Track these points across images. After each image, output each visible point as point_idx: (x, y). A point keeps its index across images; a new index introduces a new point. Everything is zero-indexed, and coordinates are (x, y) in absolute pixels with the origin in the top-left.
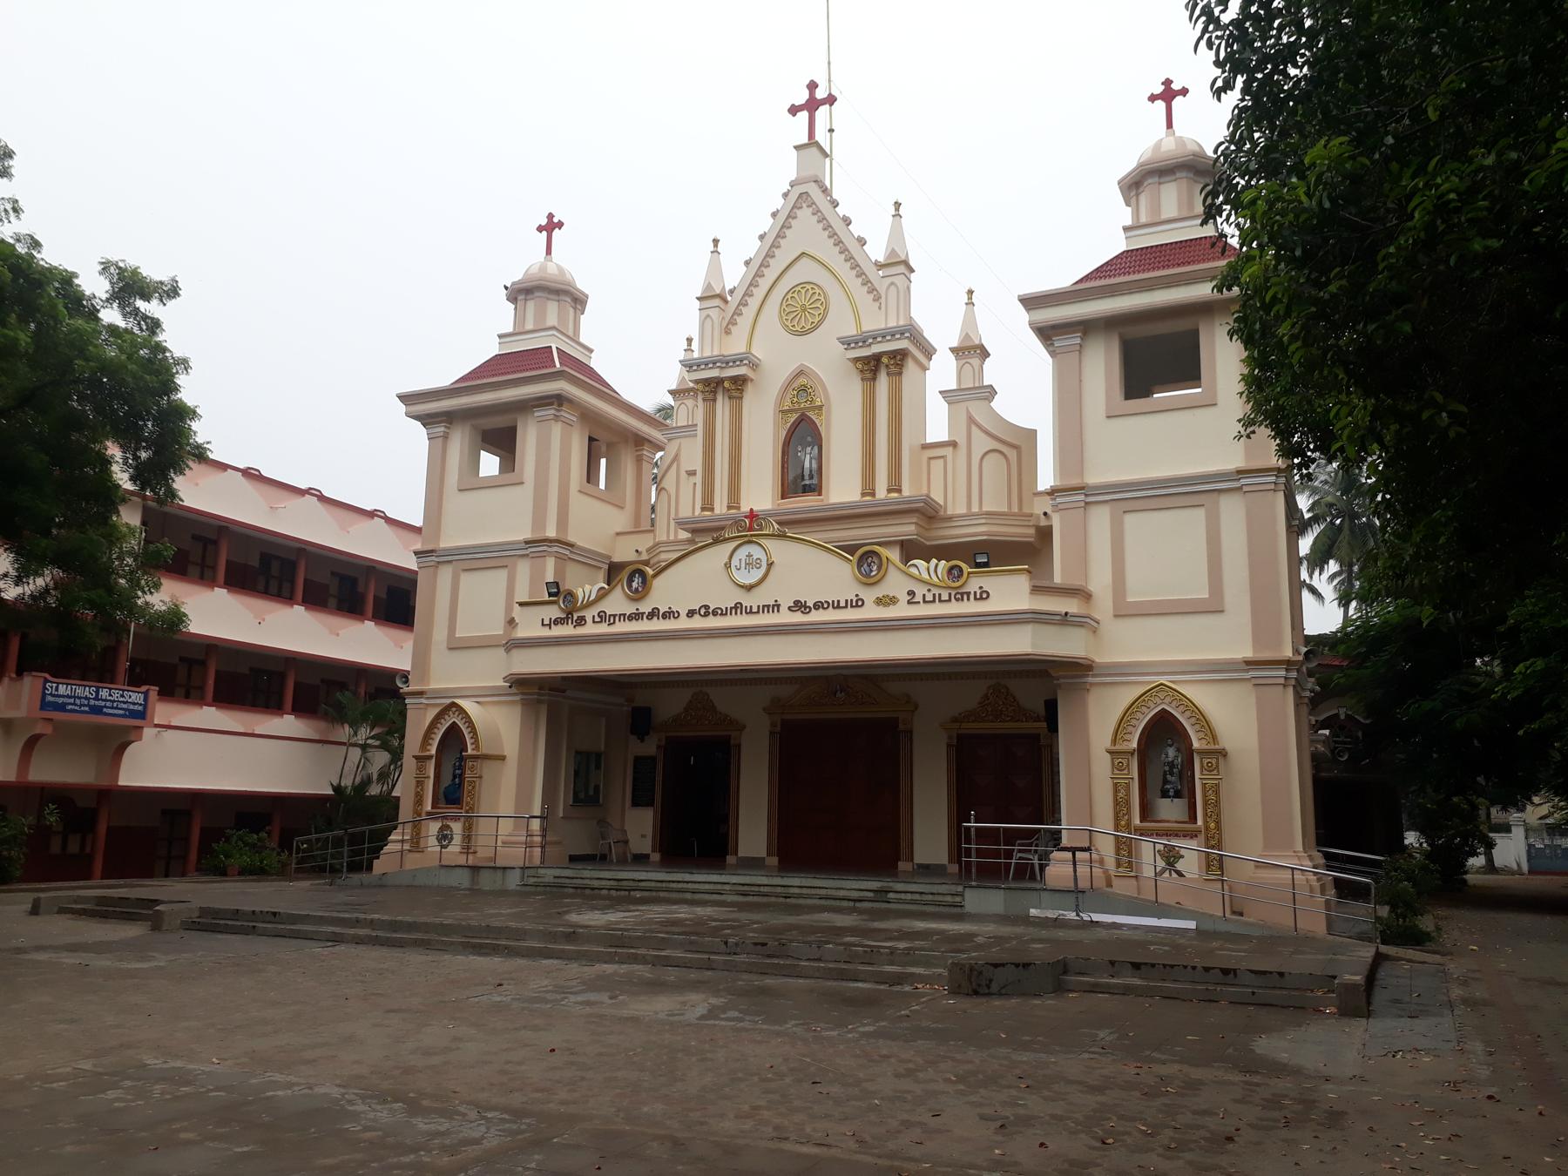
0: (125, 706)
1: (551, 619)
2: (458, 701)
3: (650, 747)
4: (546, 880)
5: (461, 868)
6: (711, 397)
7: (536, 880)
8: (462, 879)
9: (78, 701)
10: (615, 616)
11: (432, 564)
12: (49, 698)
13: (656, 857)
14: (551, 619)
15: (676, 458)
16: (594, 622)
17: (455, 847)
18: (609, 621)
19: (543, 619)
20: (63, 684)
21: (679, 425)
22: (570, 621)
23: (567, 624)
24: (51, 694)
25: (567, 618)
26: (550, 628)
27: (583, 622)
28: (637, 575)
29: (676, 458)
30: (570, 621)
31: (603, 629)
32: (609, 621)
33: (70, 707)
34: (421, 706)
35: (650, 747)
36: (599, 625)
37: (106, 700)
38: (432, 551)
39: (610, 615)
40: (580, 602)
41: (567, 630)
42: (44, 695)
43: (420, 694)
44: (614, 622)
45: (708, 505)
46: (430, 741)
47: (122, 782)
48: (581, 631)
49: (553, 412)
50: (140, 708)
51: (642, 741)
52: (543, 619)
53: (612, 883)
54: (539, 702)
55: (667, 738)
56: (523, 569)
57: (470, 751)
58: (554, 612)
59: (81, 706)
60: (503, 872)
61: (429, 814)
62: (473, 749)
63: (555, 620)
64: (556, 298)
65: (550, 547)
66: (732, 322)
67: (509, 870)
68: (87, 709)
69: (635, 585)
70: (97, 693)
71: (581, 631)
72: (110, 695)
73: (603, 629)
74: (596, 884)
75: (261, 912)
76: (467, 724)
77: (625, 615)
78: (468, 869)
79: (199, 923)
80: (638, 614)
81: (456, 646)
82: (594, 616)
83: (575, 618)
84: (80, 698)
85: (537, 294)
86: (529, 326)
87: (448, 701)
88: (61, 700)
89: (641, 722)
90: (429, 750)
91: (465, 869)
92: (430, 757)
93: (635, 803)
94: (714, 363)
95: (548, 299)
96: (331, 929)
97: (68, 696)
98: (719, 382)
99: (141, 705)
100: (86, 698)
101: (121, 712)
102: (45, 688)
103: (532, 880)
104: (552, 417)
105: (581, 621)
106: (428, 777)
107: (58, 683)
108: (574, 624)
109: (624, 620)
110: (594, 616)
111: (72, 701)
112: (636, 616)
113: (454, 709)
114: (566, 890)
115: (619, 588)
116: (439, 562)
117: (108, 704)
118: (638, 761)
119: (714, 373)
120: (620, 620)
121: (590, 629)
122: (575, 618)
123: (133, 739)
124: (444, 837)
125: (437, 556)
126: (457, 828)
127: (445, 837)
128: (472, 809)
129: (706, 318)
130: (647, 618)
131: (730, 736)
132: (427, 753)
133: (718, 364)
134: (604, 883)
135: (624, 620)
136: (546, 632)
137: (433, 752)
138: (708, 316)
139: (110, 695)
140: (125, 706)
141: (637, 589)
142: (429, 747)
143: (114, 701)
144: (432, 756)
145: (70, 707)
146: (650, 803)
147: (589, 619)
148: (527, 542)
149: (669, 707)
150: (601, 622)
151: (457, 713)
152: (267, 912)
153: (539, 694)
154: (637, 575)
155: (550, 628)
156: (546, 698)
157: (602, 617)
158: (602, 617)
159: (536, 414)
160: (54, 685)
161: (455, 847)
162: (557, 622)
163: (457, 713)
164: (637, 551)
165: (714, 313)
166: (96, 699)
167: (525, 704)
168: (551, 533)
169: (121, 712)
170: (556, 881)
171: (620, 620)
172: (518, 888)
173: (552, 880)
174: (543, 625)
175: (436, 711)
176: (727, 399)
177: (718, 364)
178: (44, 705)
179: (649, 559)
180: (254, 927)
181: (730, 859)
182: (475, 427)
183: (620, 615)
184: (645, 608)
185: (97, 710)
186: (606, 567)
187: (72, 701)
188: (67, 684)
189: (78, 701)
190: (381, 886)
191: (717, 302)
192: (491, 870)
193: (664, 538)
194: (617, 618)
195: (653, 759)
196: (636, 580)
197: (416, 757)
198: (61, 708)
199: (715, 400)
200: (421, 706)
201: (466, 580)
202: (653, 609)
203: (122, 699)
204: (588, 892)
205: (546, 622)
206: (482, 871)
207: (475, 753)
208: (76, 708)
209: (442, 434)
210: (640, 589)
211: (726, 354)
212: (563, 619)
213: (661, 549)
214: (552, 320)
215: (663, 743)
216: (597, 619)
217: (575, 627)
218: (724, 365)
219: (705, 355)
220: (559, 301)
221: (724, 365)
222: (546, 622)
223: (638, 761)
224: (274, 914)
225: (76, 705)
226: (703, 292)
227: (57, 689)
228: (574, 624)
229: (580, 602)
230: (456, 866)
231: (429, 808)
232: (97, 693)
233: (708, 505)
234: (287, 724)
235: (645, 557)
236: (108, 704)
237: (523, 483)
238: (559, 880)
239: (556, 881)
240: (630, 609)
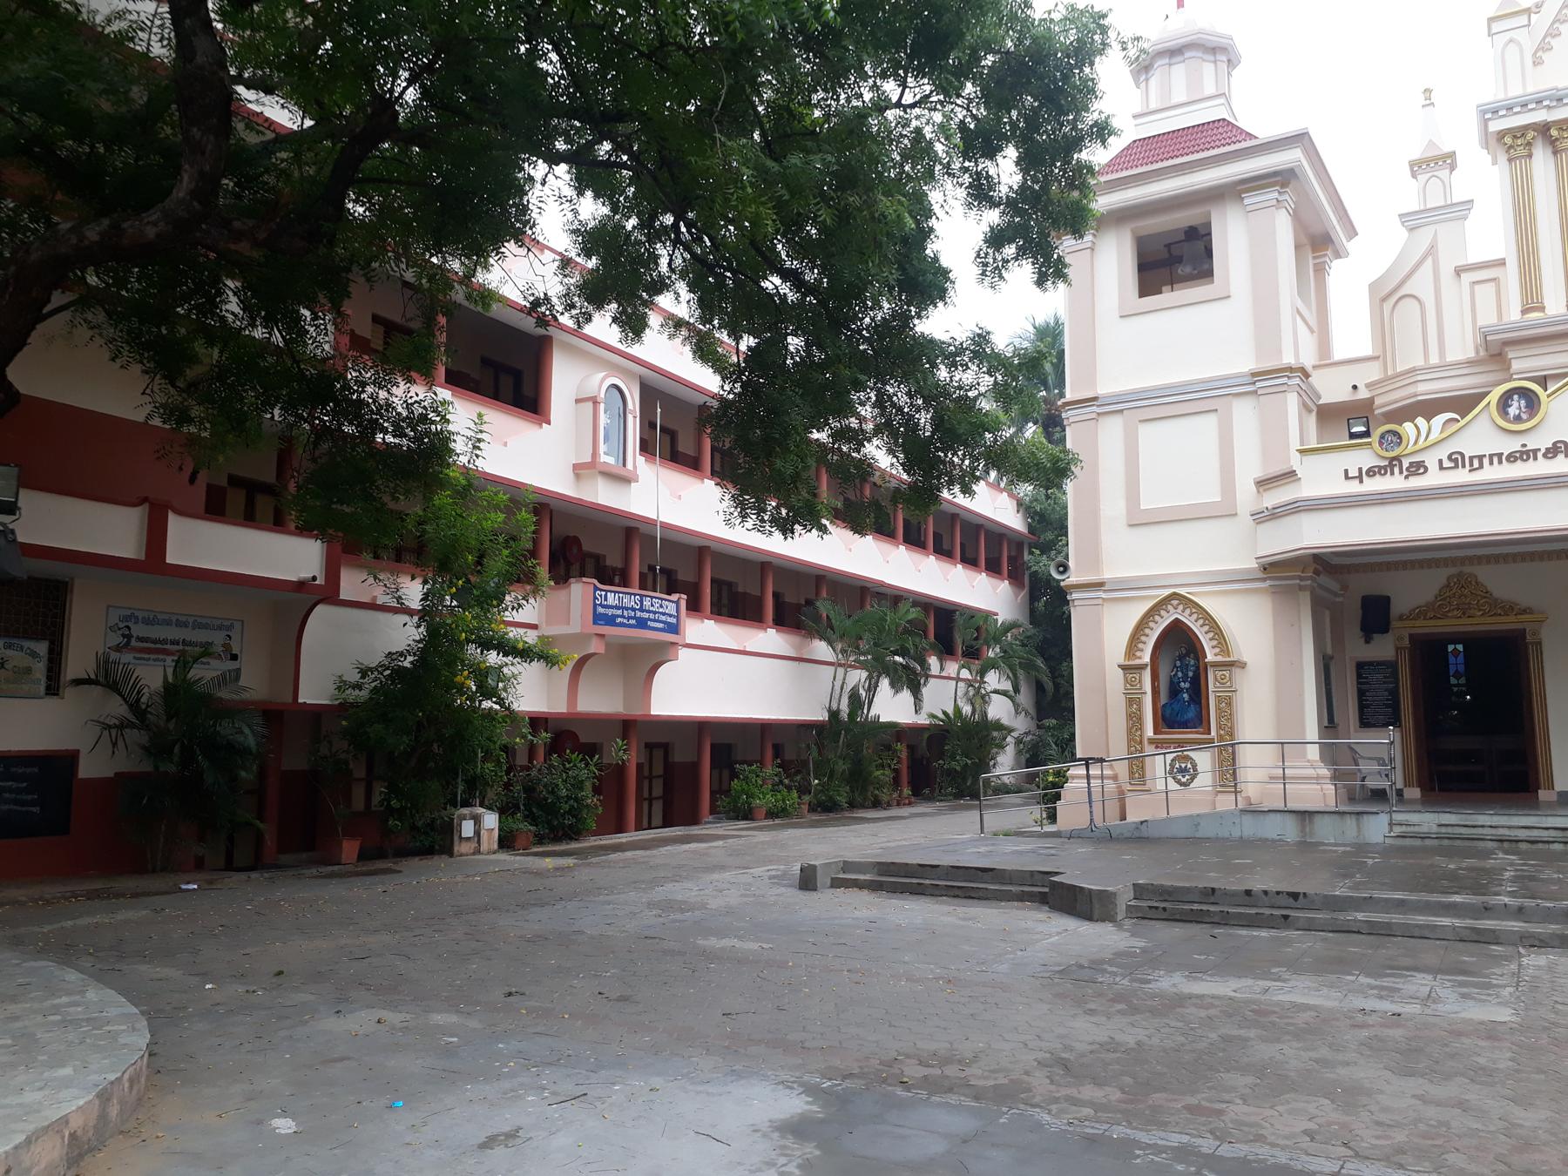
0: (663, 618)
1: (1360, 469)
2: (1177, 590)
3: (1383, 649)
4: (1425, 829)
5: (1278, 815)
6: (1525, 152)
7: (1404, 829)
8: (1289, 830)
9: (626, 613)
10: (1481, 458)
11: (1094, 416)
12: (601, 610)
13: (1414, 793)
14: (1360, 469)
15: (1432, 251)
16: (1441, 468)
17: (1204, 780)
18: (1471, 465)
19: (1346, 471)
20: (611, 592)
21: (1428, 206)
22: (1396, 470)
23: (1392, 473)
24: (601, 605)
25: (1391, 466)
26: (1361, 481)
27: (1422, 470)
28: (1516, 397)
29: (1432, 251)
30: (1396, 470)
31: (1462, 476)
32: (1471, 465)
33: (619, 620)
34: (1100, 601)
35: (1383, 649)
36: (1452, 472)
37: (649, 612)
38: (1095, 399)
39: (1471, 458)
40: (1412, 442)
41: (1394, 482)
42: (595, 605)
43: (1099, 585)
44: (1481, 466)
45: (1532, 303)
46: (1140, 646)
47: (652, 713)
48: (1416, 482)
49: (1276, 195)
50: (674, 621)
51: (1367, 641)
52: (1346, 471)
53: (1553, 833)
54: (1301, 588)
55: (1411, 636)
56: (1244, 413)
57: (1210, 657)
58: (1364, 458)
59: (629, 618)
60: (1358, 819)
61: (1151, 741)
62: (1216, 655)
63: (1368, 473)
64: (1212, 58)
65: (1289, 377)
66: (1543, 47)
67: (1365, 816)
68: (633, 622)
69: (1513, 411)
70: (641, 602)
71: (1416, 482)
72: (652, 605)
73: (1462, 476)
74: (1523, 834)
75: (1266, 893)
76: (1201, 622)
77: (1500, 455)
78: (1294, 815)
79: (1164, 909)
80: (1527, 452)
81: (1140, 521)
82: (1441, 461)
83: (1405, 464)
84: (627, 609)
85: (1188, 54)
86: (1179, 96)
87: (1167, 592)
88: (610, 612)
89: (1375, 615)
90: (1140, 658)
91: (1288, 816)
92: (1142, 667)
93: (1365, 723)
94: (1539, 102)
95: (1204, 60)
96: (1457, 922)
97: (617, 607)
98: (1544, 129)
99: (670, 616)
100: (633, 609)
101: (661, 625)
102: (595, 598)
103: (1397, 830)
104: (1274, 202)
105: (1418, 468)
106: (1145, 693)
107: (606, 591)
108: (1405, 473)
109: (1500, 462)
110: (1441, 461)
111: (619, 612)
112: (1526, 455)
113: (1175, 602)
114: (1481, 844)
115: (1484, 419)
116: (1099, 414)
117: (652, 616)
118: (1361, 666)
119: (1540, 116)
120: (1491, 463)
121: (1433, 478)
122: (1405, 464)
123: (665, 659)
124: (1183, 772)
125: (1098, 406)
126: (1204, 760)
127: (1183, 771)
128: (1231, 735)
129: (1507, 44)
130: (1545, 456)
131: (1525, 630)
132: (1137, 662)
133: (1545, 103)
134: (1535, 833)
135: (1500, 462)
136: (1354, 488)
137: (1147, 659)
138: (1511, 41)
139: (652, 605)
140: (663, 618)
141: (1518, 419)
142: (1138, 654)
143: (655, 613)
144: (1147, 665)
145: (619, 620)
146: (1395, 721)
147: (1432, 464)
148: (1254, 375)
149: (1409, 594)
150: (1456, 466)
151: (1181, 607)
152: (1278, 893)
153: (1301, 578)
154: (1516, 397)
155: (1361, 482)
156: (1309, 582)
157: (1457, 460)
158: (1457, 460)
159: (1246, 202)
160: (603, 593)
161: (1204, 780)
162: (1371, 472)
163: (1181, 607)
164: (1355, 387)
165: (1521, 35)
166: (641, 610)
167: (1276, 592)
168: (1288, 359)
169: (661, 625)
170: (1443, 830)
171: (1491, 463)
172: (1387, 841)
173: (1435, 829)
174: (1347, 477)
175: (1142, 608)
176: (1549, 150)
177: (1545, 103)
178: (598, 619)
179: (1371, 401)
180: (1286, 917)
181: (1543, 795)
182: (1133, 231)
183: (1491, 456)
184: (1541, 441)
185: (642, 624)
186: (1315, 409)
187: (619, 612)
188: (615, 592)
189: (626, 613)
190: (1140, 838)
191: (1523, 20)
192: (1336, 817)
193: (1420, 363)
194: (1486, 461)
195: (1391, 667)
196: (1515, 404)
197: (1124, 668)
198: (610, 621)
199: (1530, 156)
200: (1100, 601)
201: (1147, 433)
202: (1555, 444)
203: (661, 610)
204: (1523, 846)
205: (1353, 473)
206: (1318, 818)
207: (1219, 659)
208: (625, 621)
209: (1089, 245)
210: (1524, 416)
211: (1560, 86)
212: (1385, 467)
213: (1419, 378)
214: (1210, 89)
215: (1406, 642)
216: (1447, 464)
217: (1406, 477)
218: (1554, 104)
219: (1510, 95)
220: (1215, 62)
221: (1554, 104)
222: (1353, 473)
223: (1361, 666)
224: (1295, 896)
225: (624, 617)
226: (1497, 11)
227: (606, 600)
228: (1405, 473)
229: (1412, 442)
230: (1269, 811)
231: (1149, 731)
232: (641, 602)
233: (1532, 303)
234: (770, 639)
235: (1363, 394)
236: (652, 616)
237: (1229, 297)
238: (1450, 830)
239: (1443, 830)
240: (1512, 445)
